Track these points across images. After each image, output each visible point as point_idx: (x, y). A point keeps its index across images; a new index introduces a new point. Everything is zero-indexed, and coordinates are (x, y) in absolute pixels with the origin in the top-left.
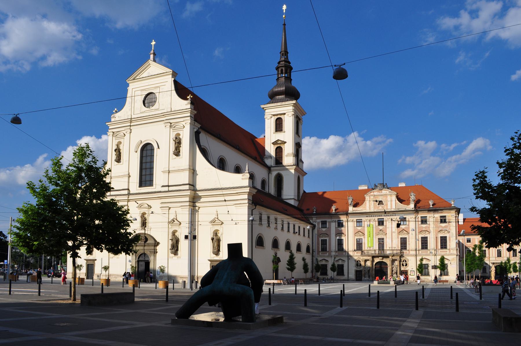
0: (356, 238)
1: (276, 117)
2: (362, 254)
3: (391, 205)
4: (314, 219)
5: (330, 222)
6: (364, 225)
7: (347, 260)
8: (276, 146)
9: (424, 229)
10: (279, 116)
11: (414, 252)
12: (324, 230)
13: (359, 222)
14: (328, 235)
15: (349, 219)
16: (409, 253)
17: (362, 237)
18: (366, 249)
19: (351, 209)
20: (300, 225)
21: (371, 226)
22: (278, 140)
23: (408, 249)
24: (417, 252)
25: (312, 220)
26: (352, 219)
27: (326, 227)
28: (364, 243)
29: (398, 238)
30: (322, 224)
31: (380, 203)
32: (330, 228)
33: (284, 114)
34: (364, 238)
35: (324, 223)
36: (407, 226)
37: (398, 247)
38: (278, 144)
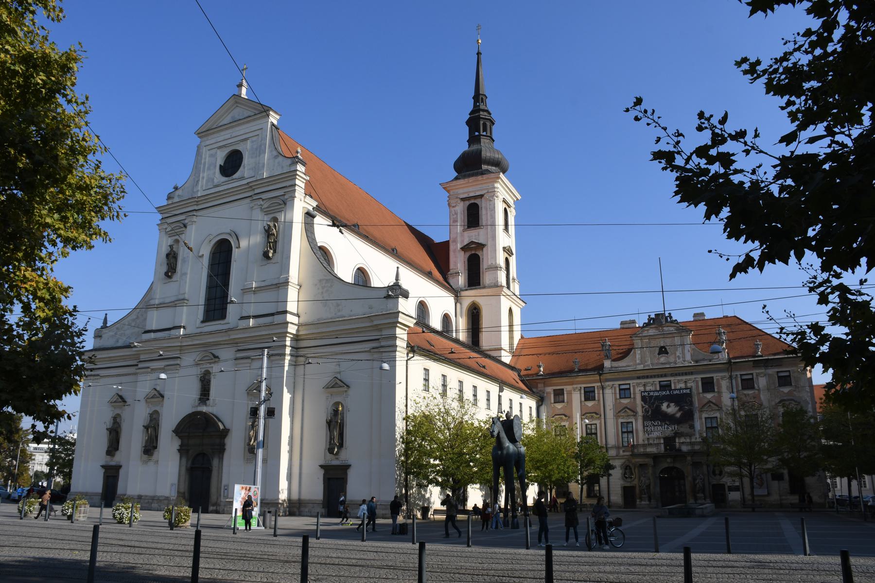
0: (620, 420)
1: (468, 203)
4: (539, 385)
5: (570, 393)
6: (634, 394)
8: (468, 254)
10: (472, 201)
12: (559, 406)
14: (569, 417)
18: (641, 442)
19: (607, 364)
20: (522, 401)
22: (472, 243)
25: (537, 387)
26: (610, 383)
27: (563, 402)
28: (637, 430)
30: (555, 395)
31: (663, 351)
32: (570, 402)
33: (481, 196)
34: (636, 420)
35: (559, 394)
36: (716, 394)
38: (471, 249)
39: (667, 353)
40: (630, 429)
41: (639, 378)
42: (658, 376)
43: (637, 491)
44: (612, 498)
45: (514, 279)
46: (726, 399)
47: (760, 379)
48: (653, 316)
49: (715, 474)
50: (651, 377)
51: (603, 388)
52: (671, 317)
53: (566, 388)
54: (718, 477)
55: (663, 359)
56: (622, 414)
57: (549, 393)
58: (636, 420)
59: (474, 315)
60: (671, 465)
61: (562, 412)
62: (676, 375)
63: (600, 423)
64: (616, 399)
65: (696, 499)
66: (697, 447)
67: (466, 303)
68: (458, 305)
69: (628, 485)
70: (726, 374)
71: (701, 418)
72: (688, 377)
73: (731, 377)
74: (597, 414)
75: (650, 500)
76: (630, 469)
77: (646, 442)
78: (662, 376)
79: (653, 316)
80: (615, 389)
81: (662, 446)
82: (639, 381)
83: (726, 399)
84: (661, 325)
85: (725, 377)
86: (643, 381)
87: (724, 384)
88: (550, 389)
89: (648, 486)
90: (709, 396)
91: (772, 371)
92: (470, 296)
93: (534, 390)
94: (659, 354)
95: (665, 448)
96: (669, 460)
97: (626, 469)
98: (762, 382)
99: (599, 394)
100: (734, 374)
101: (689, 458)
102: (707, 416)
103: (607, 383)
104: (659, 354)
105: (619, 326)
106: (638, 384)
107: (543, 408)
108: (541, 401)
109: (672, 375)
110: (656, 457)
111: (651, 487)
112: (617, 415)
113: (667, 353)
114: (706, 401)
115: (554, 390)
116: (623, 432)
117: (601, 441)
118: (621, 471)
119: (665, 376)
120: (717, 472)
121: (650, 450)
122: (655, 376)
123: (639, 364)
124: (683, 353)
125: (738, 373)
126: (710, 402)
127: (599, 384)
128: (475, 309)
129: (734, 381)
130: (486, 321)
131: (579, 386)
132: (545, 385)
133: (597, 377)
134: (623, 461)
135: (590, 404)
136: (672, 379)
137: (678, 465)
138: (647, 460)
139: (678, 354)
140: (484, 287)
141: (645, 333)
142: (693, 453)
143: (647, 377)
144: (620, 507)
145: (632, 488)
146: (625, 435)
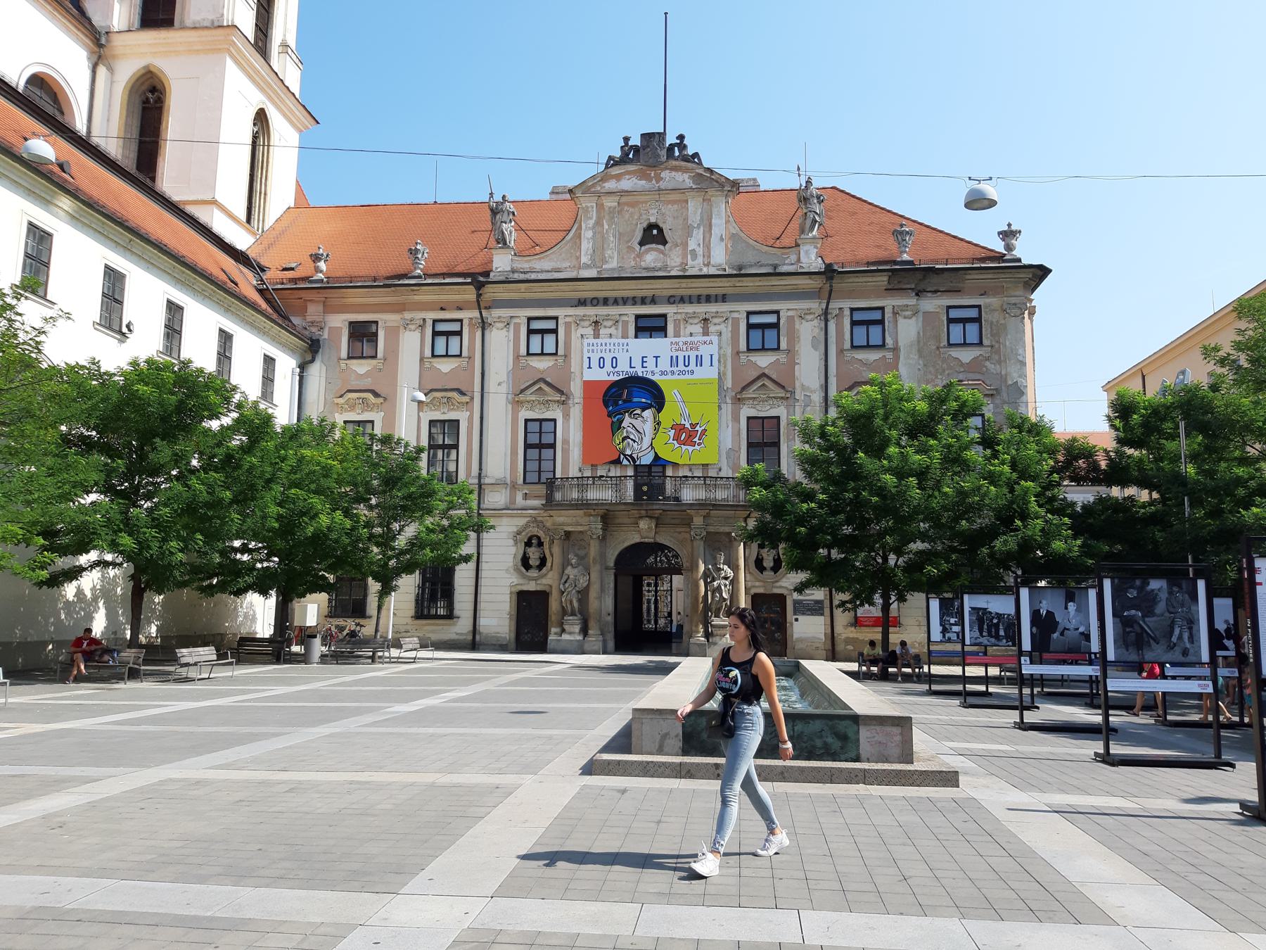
0: (525, 414)
2: (549, 499)
4: (312, 309)
5: (393, 333)
12: (362, 367)
14: (379, 395)
17: (557, 413)
18: (573, 472)
25: (303, 311)
28: (566, 442)
29: (736, 418)
31: (653, 235)
34: (566, 416)
35: (362, 334)
36: (782, 357)
37: (735, 467)
39: (664, 242)
40: (547, 439)
41: (582, 303)
42: (634, 301)
43: (554, 605)
44: (483, 622)
45: (285, 45)
46: (808, 371)
47: (901, 321)
48: (636, 141)
50: (616, 302)
51: (484, 325)
52: (682, 146)
53: (386, 320)
55: (651, 257)
56: (529, 396)
57: (335, 331)
58: (566, 416)
59: (149, 103)
61: (367, 383)
62: (682, 300)
63: (470, 419)
64: (517, 357)
66: (721, 495)
67: (127, 70)
68: (102, 70)
69: (531, 587)
70: (816, 306)
71: (736, 418)
72: (712, 308)
73: (826, 313)
74: (462, 393)
76: (540, 544)
77: (588, 473)
78: (643, 301)
79: (636, 141)
80: (517, 326)
81: (630, 484)
82: (581, 311)
83: (808, 371)
84: (656, 165)
85: (809, 312)
86: (591, 311)
87: (808, 330)
88: (339, 322)
89: (584, 594)
90: (764, 361)
91: (933, 304)
92: (140, 50)
93: (296, 320)
94: (641, 244)
95: (637, 488)
96: (643, 524)
97: (528, 544)
98: (906, 331)
99: (472, 340)
100: (835, 305)
102: (753, 413)
103: (496, 313)
104: (641, 244)
105: (547, 197)
106: (579, 321)
107: (316, 372)
108: (310, 349)
109: (671, 300)
110: (608, 516)
111: (593, 594)
112: (517, 398)
113: (664, 242)
114: (755, 374)
115: (351, 323)
116: (527, 446)
117: (464, 466)
118: (513, 550)
119: (654, 301)
121: (593, 495)
122: (625, 301)
123: (587, 267)
124: (707, 246)
125: (847, 304)
126: (764, 375)
127: (476, 314)
128: (153, 90)
129: (832, 326)
130: (174, 125)
131: (420, 315)
132: (328, 309)
133: (470, 294)
135: (445, 366)
139: (692, 245)
140: (183, 28)
141: (611, 185)
142: (706, 506)
143: (605, 302)
144: (503, 648)
145: (543, 596)
146: (533, 453)
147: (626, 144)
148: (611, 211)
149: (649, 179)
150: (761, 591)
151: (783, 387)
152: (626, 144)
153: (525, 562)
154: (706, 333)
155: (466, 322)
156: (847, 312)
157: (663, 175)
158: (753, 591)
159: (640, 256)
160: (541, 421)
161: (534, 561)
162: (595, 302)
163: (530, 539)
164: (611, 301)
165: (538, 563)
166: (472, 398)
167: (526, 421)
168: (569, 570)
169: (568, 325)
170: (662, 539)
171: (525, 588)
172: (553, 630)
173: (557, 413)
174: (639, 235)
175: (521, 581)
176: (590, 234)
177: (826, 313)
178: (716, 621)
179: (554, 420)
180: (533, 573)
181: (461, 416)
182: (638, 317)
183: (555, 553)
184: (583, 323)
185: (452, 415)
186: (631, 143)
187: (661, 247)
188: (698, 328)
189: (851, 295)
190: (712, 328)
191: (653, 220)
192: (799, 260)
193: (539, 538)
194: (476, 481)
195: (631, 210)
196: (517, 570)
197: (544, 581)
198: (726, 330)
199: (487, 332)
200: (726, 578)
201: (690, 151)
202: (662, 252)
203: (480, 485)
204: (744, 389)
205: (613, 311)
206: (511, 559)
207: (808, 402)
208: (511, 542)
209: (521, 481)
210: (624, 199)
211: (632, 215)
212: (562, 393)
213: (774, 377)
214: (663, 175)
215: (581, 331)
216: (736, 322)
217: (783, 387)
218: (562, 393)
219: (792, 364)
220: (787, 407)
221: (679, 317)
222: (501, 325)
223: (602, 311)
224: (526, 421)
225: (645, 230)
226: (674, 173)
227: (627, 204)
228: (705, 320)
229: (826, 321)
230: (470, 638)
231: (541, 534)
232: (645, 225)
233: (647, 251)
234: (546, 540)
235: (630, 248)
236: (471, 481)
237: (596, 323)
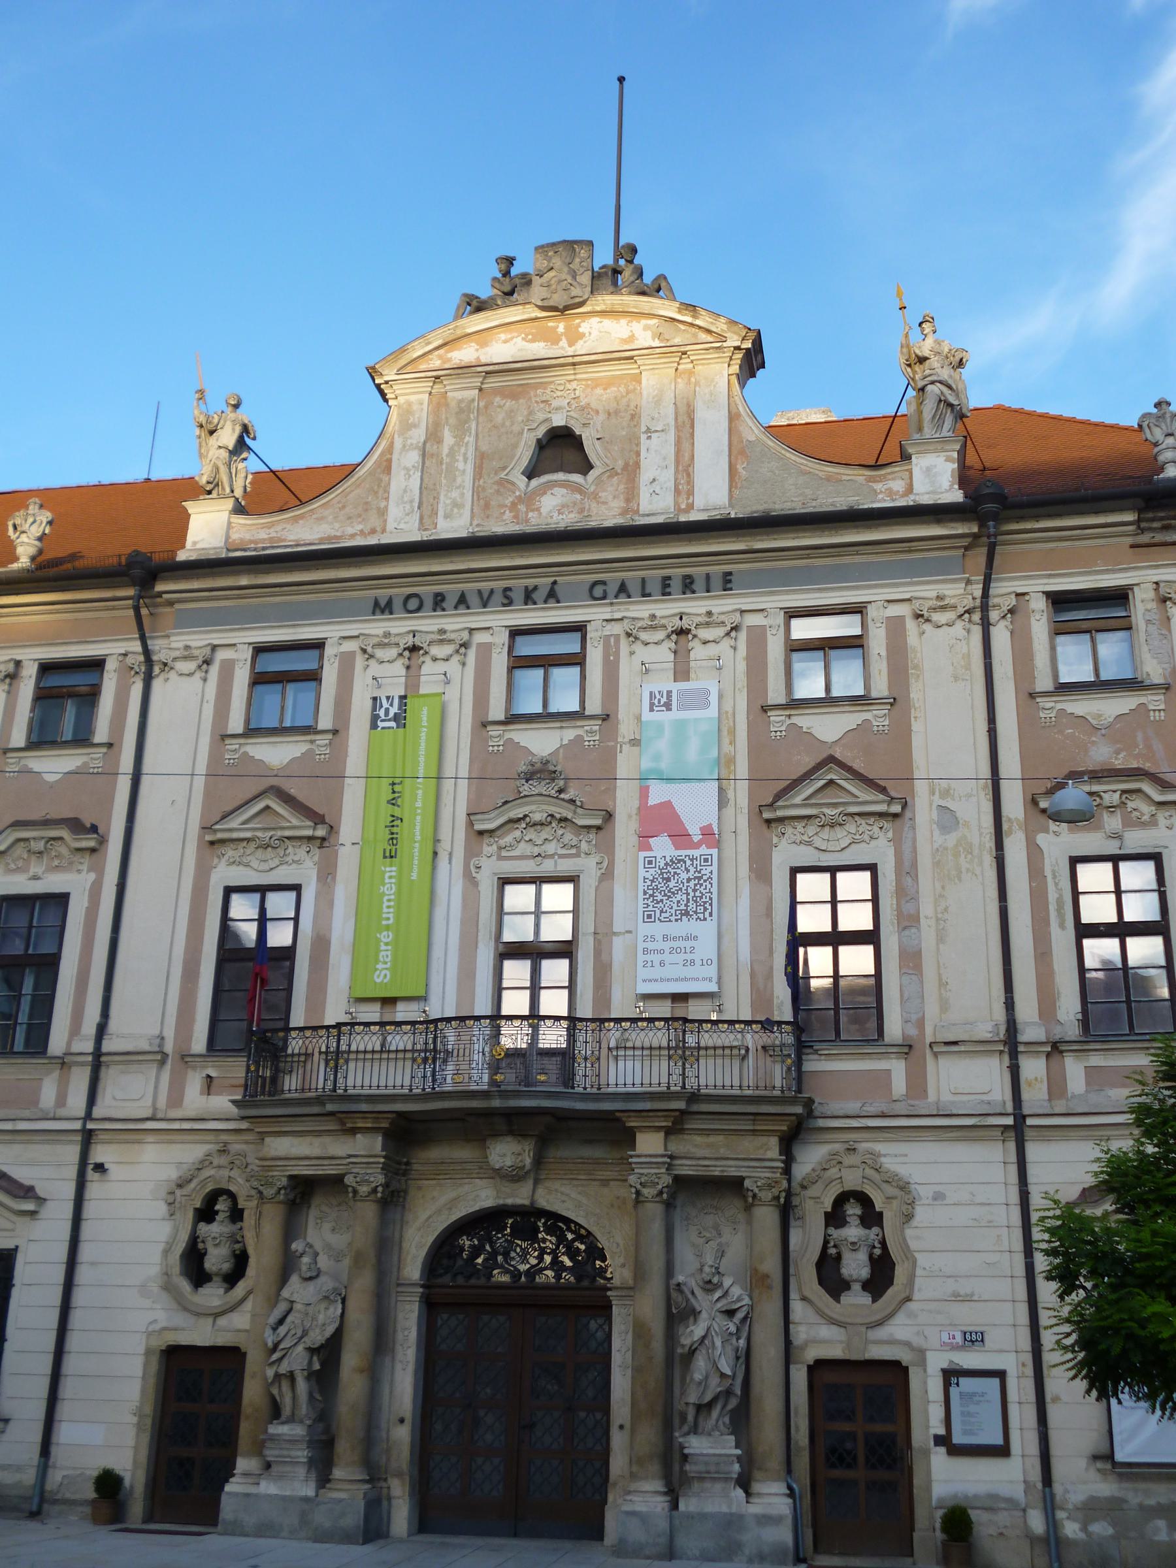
0: (225, 873)
3: (684, 466)
7: (56, 1183)
9: (1101, 754)
11: (977, 1082)
13: (284, 671)
15: (171, 644)
16: (917, 1083)
21: (422, 715)
23: (894, 1028)
24: (1033, 1068)
26: (198, 640)
34: (327, 874)
39: (585, 467)
41: (383, 608)
49: (831, 1278)
54: (856, 1298)
60: (520, 1196)
65: (676, 1476)
69: (201, 1335)
70: (959, 591)
74: (76, 825)
75: (322, 1464)
76: (236, 1215)
80: (228, 669)
82: (377, 627)
86: (400, 626)
89: (329, 1352)
94: (531, 473)
97: (206, 1214)
101: (649, 1144)
104: (531, 473)
109: (596, 593)
111: (351, 1360)
113: (585, 467)
114: (807, 761)
120: (856, 1266)
129: (1001, 636)
134: (191, 1153)
136: (593, 614)
137: (561, 1196)
138: (340, 1147)
147: (506, 274)
148: (463, 410)
149: (554, 340)
150: (836, 1352)
151: (883, 790)
152: (506, 274)
153: (194, 1265)
154: (682, 672)
155: (111, 665)
156: (1039, 604)
157: (584, 327)
158: (812, 1354)
159: (529, 499)
160: (263, 890)
161: (217, 1259)
162: (413, 605)
163: (212, 1198)
164: (451, 600)
165: (226, 1267)
166: (103, 841)
167: (229, 891)
168: (295, 1289)
169: (347, 662)
170: (548, 1199)
171: (185, 1339)
172: (243, 1464)
173: (302, 867)
174: (525, 454)
175: (180, 1319)
176: (414, 457)
177: (985, 608)
178: (696, 1445)
179: (297, 888)
180: (212, 1295)
181: (71, 881)
182: (516, 633)
183: (262, 1237)
184: (379, 653)
185: (53, 883)
186: (514, 271)
187: (576, 478)
188: (663, 654)
189: (1049, 564)
190: (698, 652)
191: (558, 421)
192: (910, 489)
193: (232, 1196)
194: (89, 1047)
195: (509, 403)
196: (168, 1287)
197: (240, 1320)
198: (734, 657)
199: (157, 685)
200: (730, 1313)
201: (648, 278)
202: (578, 489)
203: (98, 1054)
204: (778, 796)
205: (454, 623)
206: (157, 1258)
207: (948, 820)
208: (162, 1208)
209: (199, 1044)
210: (493, 382)
211: (511, 414)
212: (318, 819)
213: (857, 765)
214: (584, 327)
215: (375, 669)
216: (758, 639)
217: (883, 790)
218: (318, 819)
219: (901, 734)
220: (897, 842)
221: (617, 629)
222: (191, 666)
223: (427, 624)
224: (229, 891)
225: (541, 445)
226: (608, 323)
227: (497, 391)
228: (682, 632)
229: (986, 625)
230: (29, 1477)
231: (240, 1186)
232: (541, 432)
233: (544, 490)
234: (248, 1205)
235: (505, 484)
236: (77, 1047)
237: (414, 649)
